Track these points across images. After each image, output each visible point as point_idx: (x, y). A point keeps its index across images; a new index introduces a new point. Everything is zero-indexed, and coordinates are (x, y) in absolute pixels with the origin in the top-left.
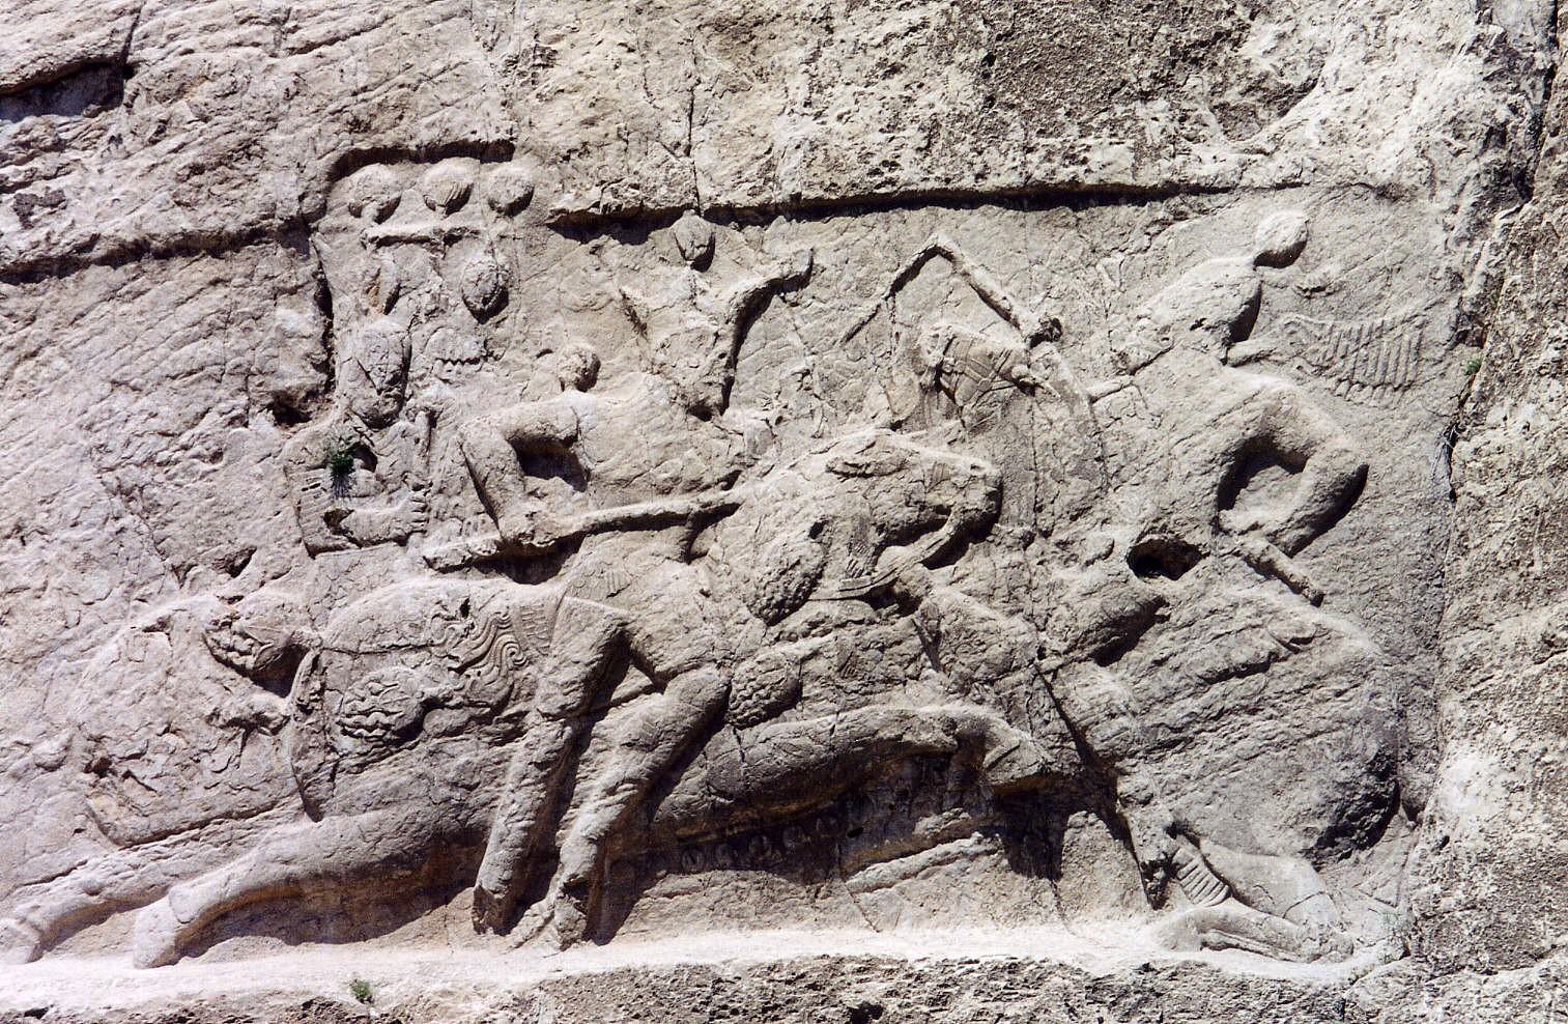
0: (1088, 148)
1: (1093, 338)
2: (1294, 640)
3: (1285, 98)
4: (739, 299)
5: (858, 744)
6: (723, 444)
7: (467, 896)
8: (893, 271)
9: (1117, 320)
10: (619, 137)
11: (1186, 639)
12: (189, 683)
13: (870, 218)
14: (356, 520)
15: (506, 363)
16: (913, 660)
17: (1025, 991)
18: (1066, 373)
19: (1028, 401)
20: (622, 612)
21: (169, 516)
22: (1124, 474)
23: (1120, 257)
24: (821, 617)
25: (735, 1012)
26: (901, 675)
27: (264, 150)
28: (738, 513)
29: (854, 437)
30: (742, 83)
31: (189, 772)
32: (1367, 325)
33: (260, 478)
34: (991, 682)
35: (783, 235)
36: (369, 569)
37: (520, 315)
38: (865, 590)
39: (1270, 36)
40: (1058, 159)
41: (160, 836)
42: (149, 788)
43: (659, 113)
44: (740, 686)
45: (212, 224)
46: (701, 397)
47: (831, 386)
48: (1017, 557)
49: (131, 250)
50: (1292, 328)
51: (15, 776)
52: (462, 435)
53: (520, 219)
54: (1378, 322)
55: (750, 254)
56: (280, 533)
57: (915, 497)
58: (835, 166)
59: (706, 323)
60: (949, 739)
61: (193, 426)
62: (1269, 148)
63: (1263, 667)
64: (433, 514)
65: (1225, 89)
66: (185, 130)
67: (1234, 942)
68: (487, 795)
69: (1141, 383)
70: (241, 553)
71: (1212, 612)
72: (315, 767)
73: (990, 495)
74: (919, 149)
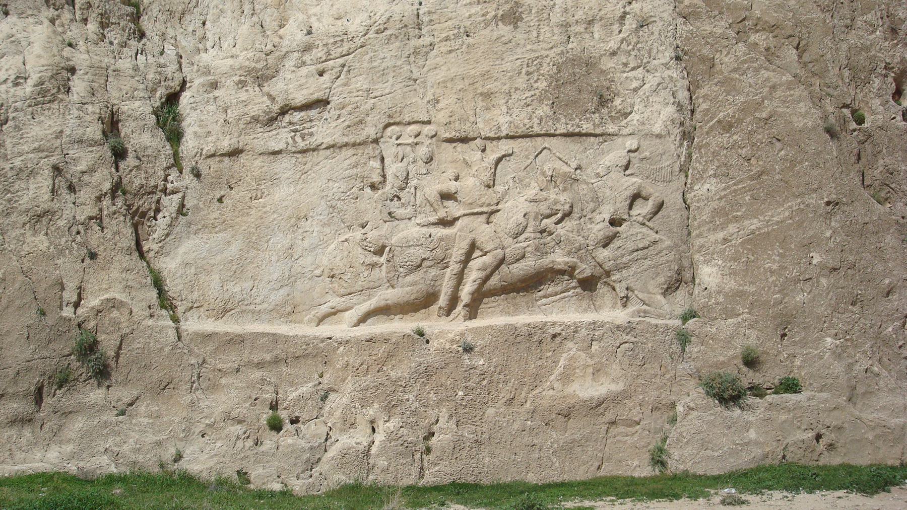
3: (626, 115)
4: (495, 159)
18: (585, 178)
20: (474, 236)
23: (592, 150)
29: (531, 192)
31: (357, 278)
33: (369, 204)
36: (402, 226)
40: (575, 127)
41: (350, 294)
47: (521, 181)
48: (578, 222)
53: (434, 139)
55: (495, 149)
58: (517, 127)
62: (626, 126)
73: (570, 207)
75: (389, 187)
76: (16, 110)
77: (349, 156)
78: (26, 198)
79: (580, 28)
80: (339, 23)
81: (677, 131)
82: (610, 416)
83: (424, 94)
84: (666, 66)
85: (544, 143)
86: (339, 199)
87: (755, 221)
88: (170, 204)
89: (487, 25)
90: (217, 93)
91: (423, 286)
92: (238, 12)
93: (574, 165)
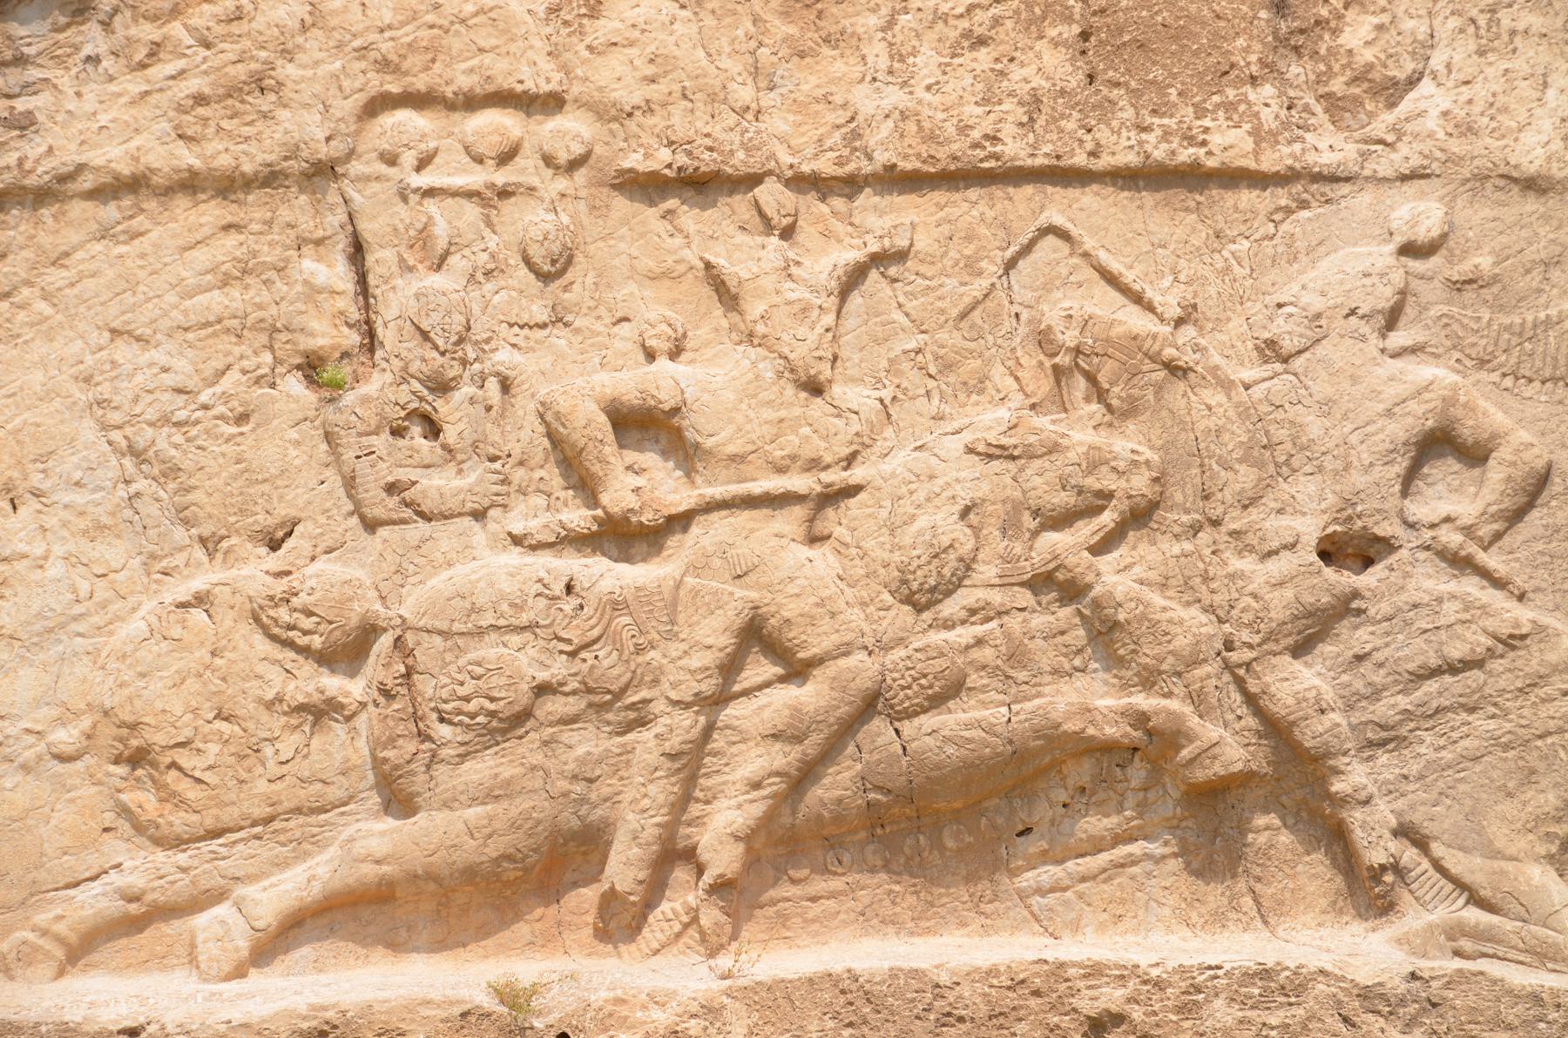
0: (1206, 130)
1: (1230, 325)
2: (1512, 636)
3: (1393, 91)
4: (840, 271)
5: (1038, 738)
6: (839, 423)
7: (589, 895)
8: (1003, 249)
9: (1254, 308)
10: (685, 96)
11: (1387, 634)
12: (242, 665)
13: (973, 193)
14: (423, 492)
15: (578, 331)
16: (1080, 651)
17: (1283, 999)
18: (1216, 359)
19: (1181, 386)
20: (754, 595)
21: (192, 482)
22: (1295, 463)
23: (1247, 244)
24: (982, 604)
25: (961, 1019)
26: (1067, 667)
27: (280, 84)
28: (862, 496)
30: (811, 48)
31: (246, 763)
32: (1530, 318)
33: (297, 443)
34: (1179, 674)
35: (875, 208)
36: (444, 545)
37: (590, 280)
38: (1026, 577)
39: (1368, 27)
42: (199, 781)
43: (723, 76)
44: (896, 675)
45: (224, 161)
46: (812, 372)
48: (1188, 546)
49: (126, 184)
50: (1445, 320)
51: (26, 768)
52: (543, 404)
53: (581, 176)
54: (1542, 316)
55: (839, 227)
56: (328, 505)
57: (1073, 482)
58: (931, 138)
59: (808, 296)
60: (1134, 734)
61: (214, 384)
62: (1390, 138)
63: (1479, 664)
64: (514, 488)
65: (1330, 78)
66: (185, 55)
67: (1491, 951)
68: (609, 790)
69: (1300, 370)
70: (282, 525)
71: (1415, 606)
72: (408, 757)
73: (1156, 480)
74: (1021, 124)
75: (389, 377)
77: (207, 231)
85: (1042, 208)
86: (165, 420)
91: (539, 800)
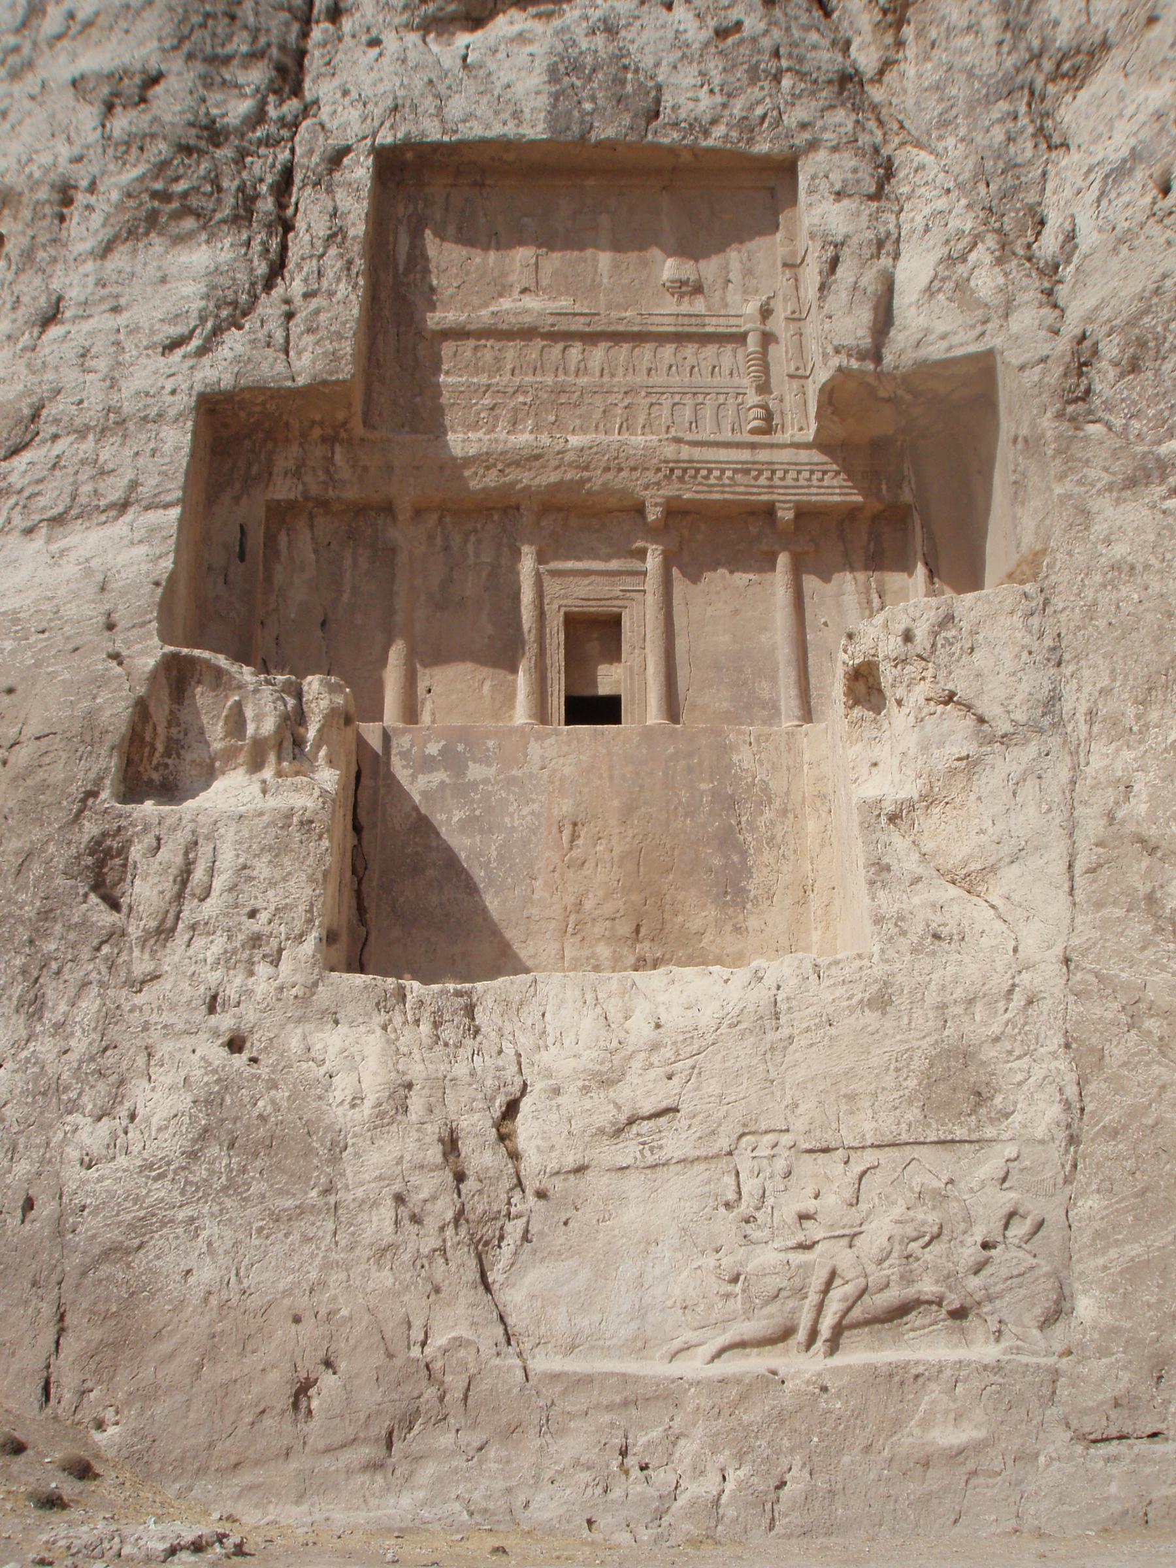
3: (1007, 1115)
76: (355, 1136)
78: (369, 1232)
79: (958, 1010)
80: (689, 1013)
81: (1062, 1135)
82: (971, 1465)
83: (783, 1097)
84: (1054, 1055)
87: (1136, 1246)
88: (514, 1230)
89: (852, 1013)
90: (560, 1100)
92: (580, 1003)
93: (945, 1179)
